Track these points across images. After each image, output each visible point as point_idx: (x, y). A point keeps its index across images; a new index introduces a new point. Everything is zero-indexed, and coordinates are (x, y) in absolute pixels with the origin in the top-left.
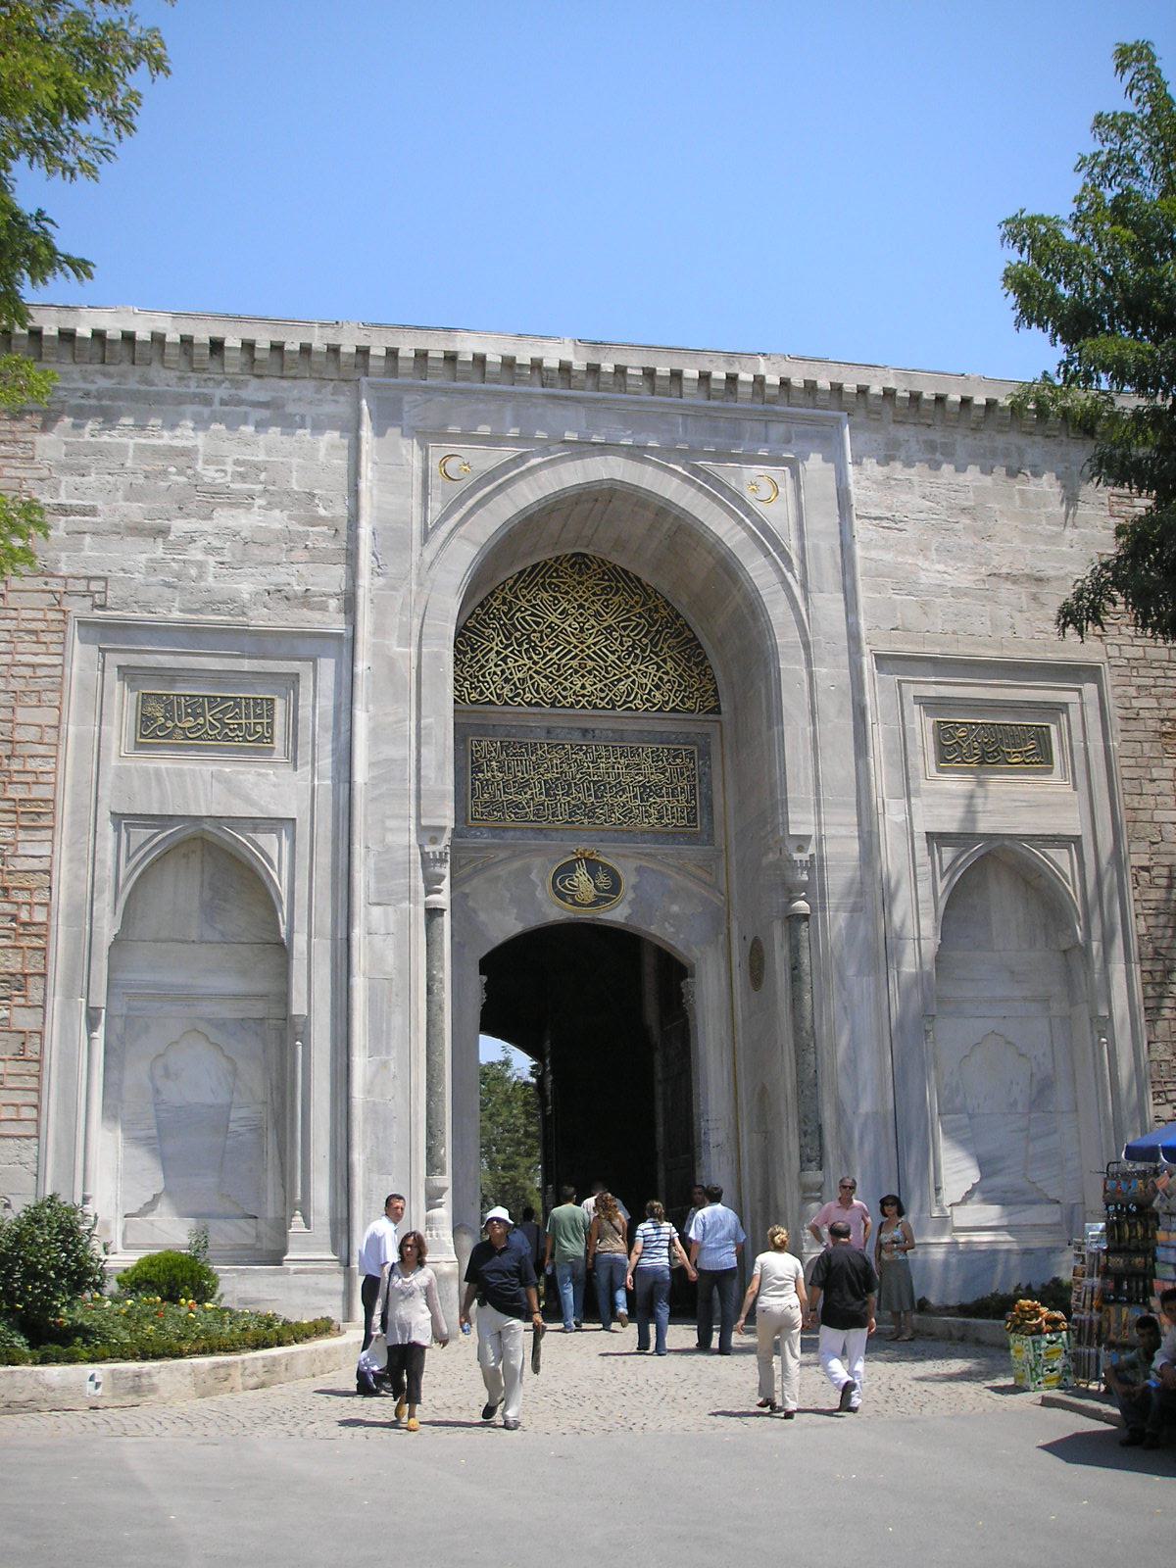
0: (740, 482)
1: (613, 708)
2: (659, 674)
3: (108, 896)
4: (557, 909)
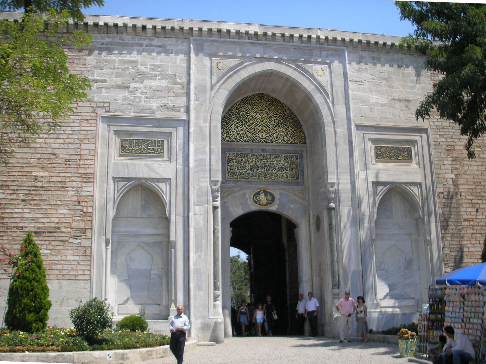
1: (272, 142)
2: (287, 131)
3: (111, 203)
4: (254, 206)
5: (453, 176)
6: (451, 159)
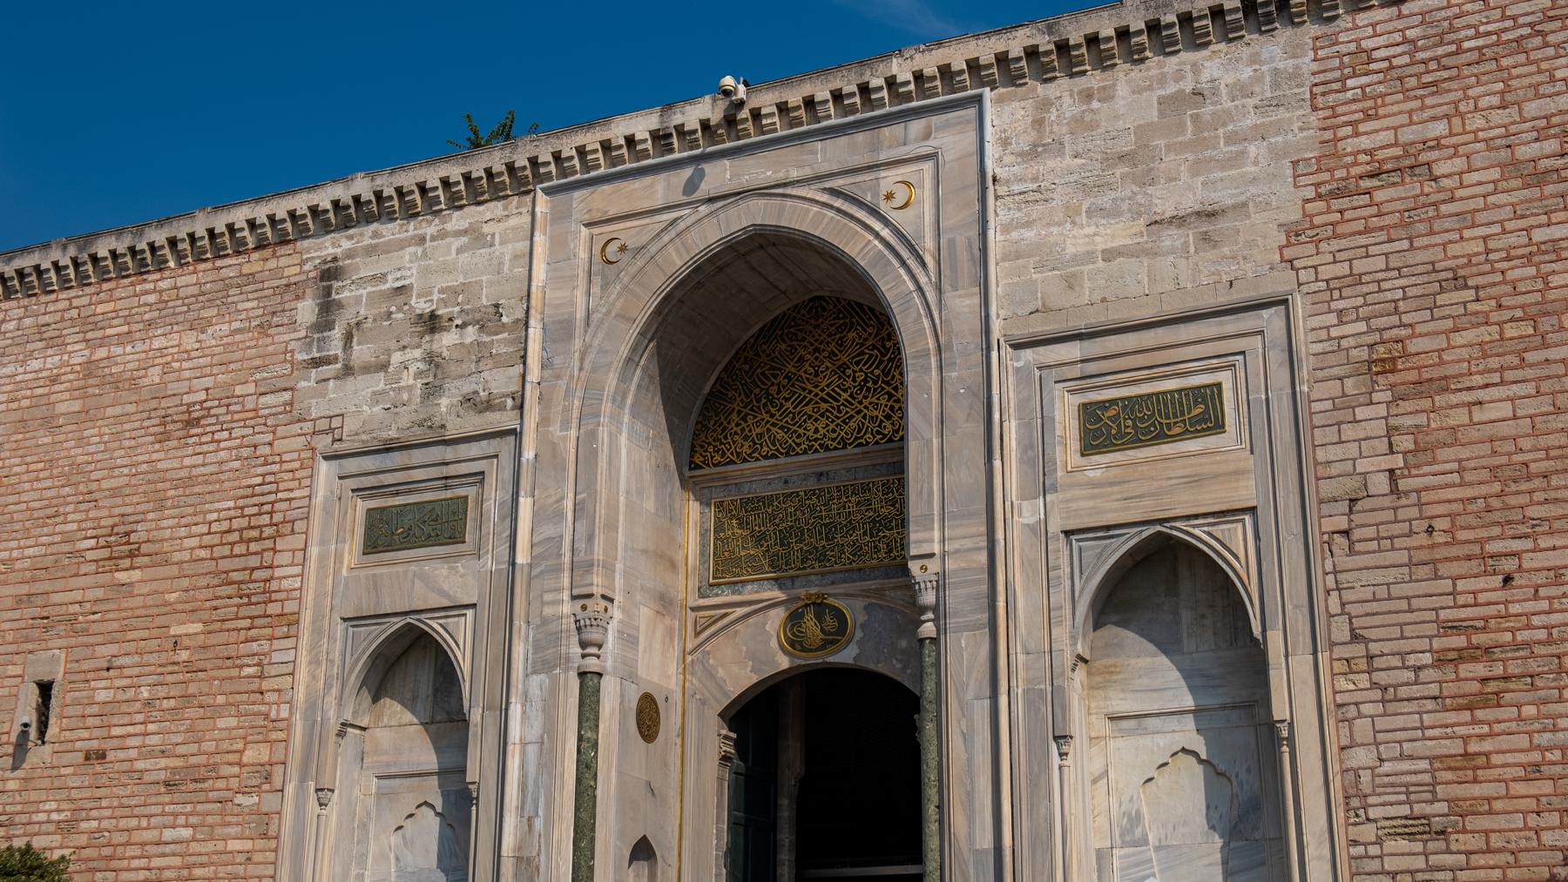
0: (876, 194)
6: (1387, 396)
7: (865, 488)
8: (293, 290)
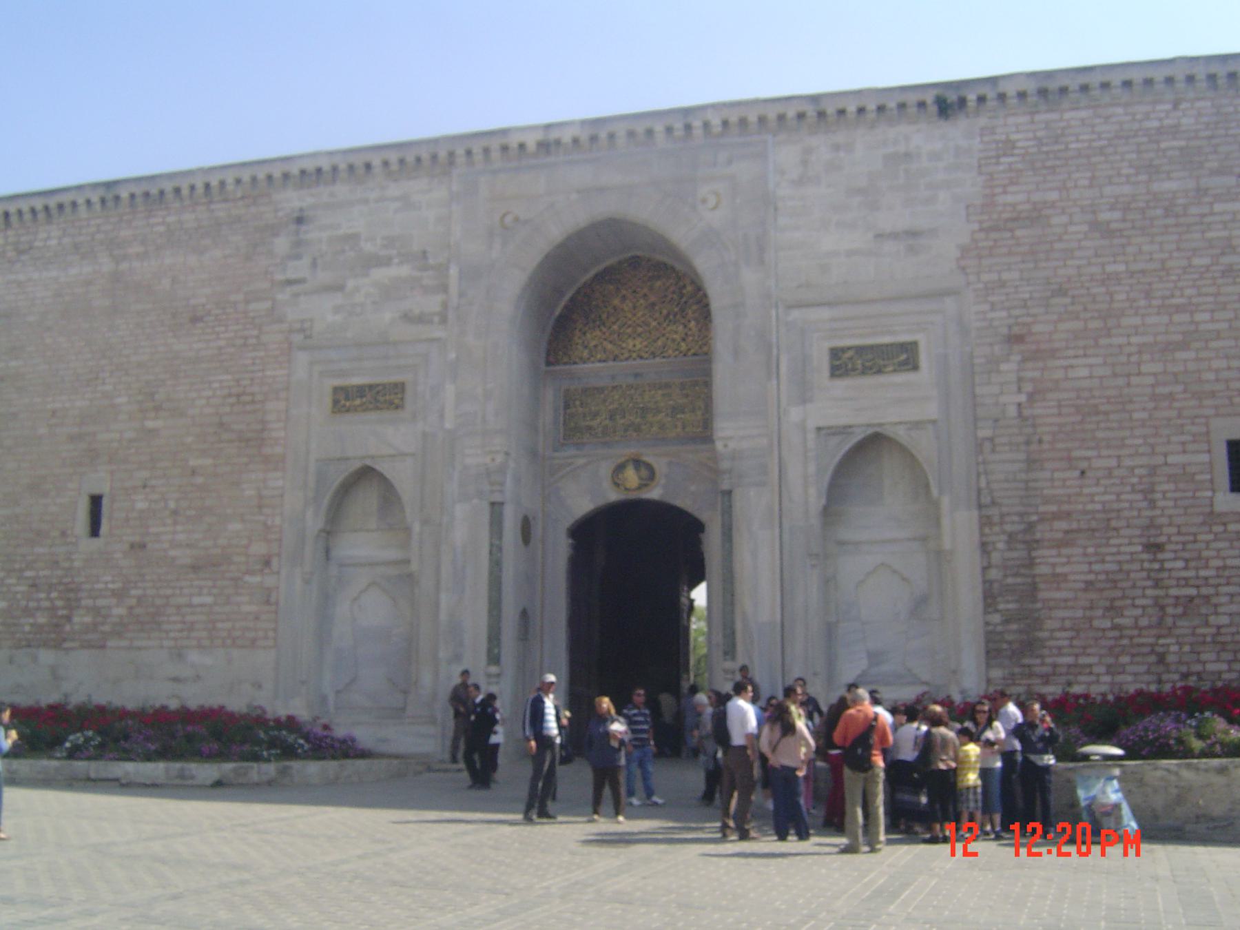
5: (1023, 398)
6: (1018, 358)
7: (667, 386)
8: (273, 230)
